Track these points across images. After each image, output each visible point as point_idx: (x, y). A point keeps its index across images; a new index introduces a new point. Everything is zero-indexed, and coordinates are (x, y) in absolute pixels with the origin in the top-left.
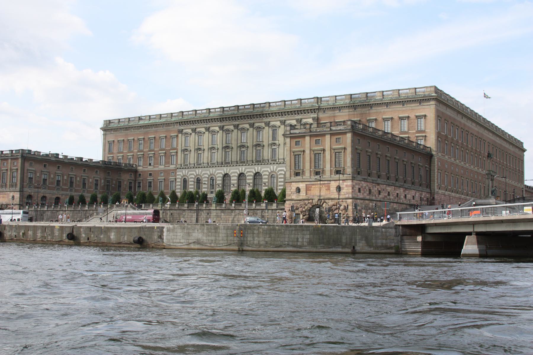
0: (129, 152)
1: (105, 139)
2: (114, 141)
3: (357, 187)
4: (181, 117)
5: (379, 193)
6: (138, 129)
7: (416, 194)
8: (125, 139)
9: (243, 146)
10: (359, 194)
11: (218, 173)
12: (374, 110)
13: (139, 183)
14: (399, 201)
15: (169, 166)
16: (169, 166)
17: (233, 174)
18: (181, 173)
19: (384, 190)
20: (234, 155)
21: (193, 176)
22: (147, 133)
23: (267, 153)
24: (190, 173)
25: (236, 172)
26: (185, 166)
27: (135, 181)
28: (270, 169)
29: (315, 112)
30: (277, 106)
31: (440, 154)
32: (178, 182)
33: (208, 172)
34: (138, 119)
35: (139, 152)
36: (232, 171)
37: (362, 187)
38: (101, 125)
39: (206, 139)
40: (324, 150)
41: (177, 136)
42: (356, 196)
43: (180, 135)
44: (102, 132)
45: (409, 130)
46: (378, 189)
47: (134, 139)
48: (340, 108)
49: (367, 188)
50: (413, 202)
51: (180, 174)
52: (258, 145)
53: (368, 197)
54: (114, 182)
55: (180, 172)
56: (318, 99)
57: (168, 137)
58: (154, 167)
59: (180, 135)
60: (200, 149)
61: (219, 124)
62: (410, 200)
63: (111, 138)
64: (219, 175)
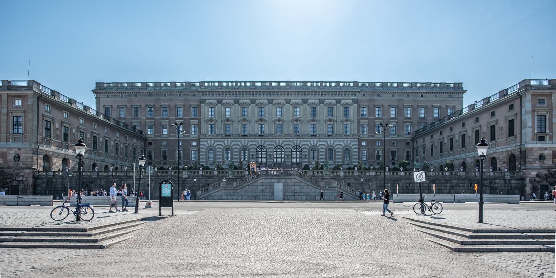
0: (133, 119)
2: (112, 106)
8: (128, 105)
11: (251, 145)
13: (150, 152)
15: (189, 136)
16: (189, 136)
18: (206, 143)
21: (221, 147)
22: (157, 100)
24: (216, 143)
25: (273, 145)
26: (211, 136)
27: (145, 149)
28: (311, 144)
29: (355, 95)
32: (203, 152)
33: (239, 143)
35: (148, 119)
36: (267, 143)
38: (94, 87)
41: (199, 106)
43: (203, 105)
47: (140, 106)
51: (205, 143)
52: (297, 120)
55: (205, 141)
56: (356, 83)
57: (187, 106)
58: (169, 136)
59: (203, 105)
63: (107, 102)
64: (251, 147)
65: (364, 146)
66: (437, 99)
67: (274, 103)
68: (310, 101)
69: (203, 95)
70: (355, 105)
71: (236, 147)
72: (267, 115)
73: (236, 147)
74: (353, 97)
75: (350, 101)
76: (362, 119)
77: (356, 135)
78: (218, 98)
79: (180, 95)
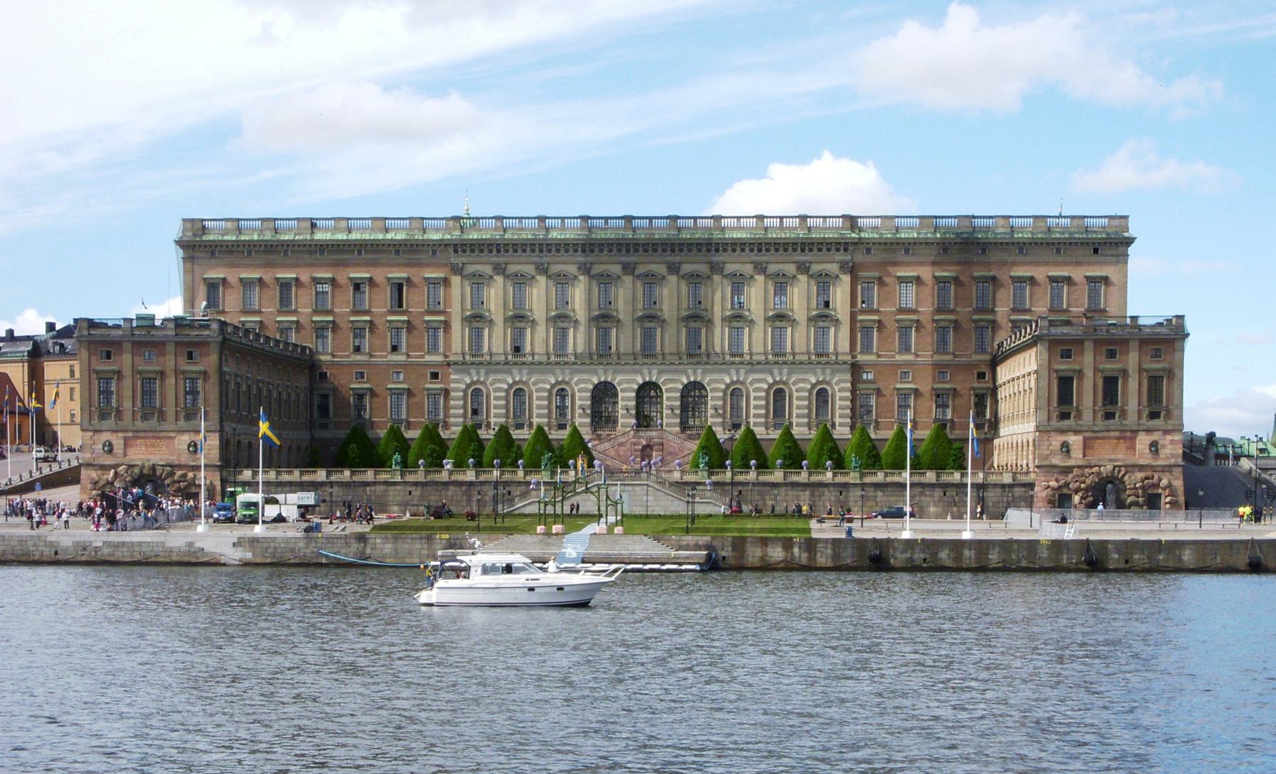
4: (458, 233)
6: (311, 253)
9: (651, 318)
12: (994, 256)
17: (625, 386)
20: (624, 339)
23: (720, 338)
26: (475, 358)
30: (740, 228)
34: (308, 224)
36: (618, 378)
39: (539, 296)
43: (456, 280)
48: (908, 247)
59: (456, 280)
60: (520, 317)
61: (581, 259)
65: (868, 382)
66: (1060, 259)
67: (637, 272)
68: (730, 268)
69: (456, 251)
70: (846, 279)
71: (541, 385)
72: (621, 305)
73: (541, 385)
74: (840, 257)
75: (833, 268)
76: (863, 312)
77: (844, 354)
78: (494, 259)
79: (397, 252)
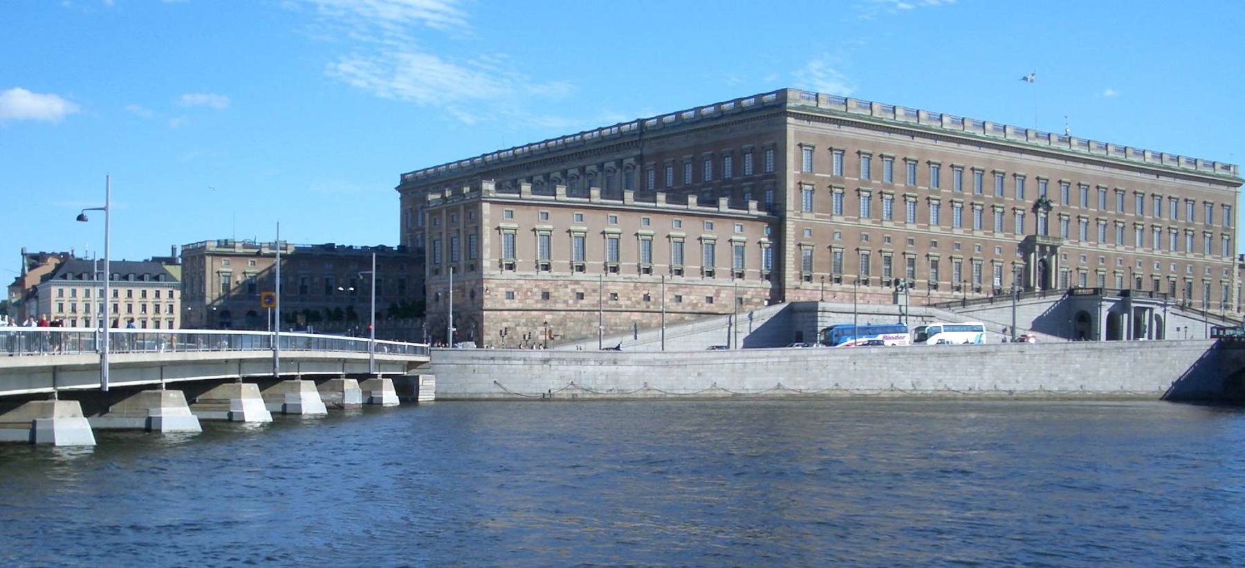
1: (402, 206)
3: (503, 290)
5: (581, 296)
7: (718, 293)
10: (507, 301)
14: (652, 308)
19: (594, 291)
31: (807, 216)
37: (518, 290)
40: (458, 231)
42: (498, 306)
44: (399, 195)
45: (754, 172)
46: (573, 290)
49: (535, 290)
50: (706, 307)
53: (539, 306)
54: (390, 281)
62: (696, 305)
70: (638, 167)
75: (632, 160)
